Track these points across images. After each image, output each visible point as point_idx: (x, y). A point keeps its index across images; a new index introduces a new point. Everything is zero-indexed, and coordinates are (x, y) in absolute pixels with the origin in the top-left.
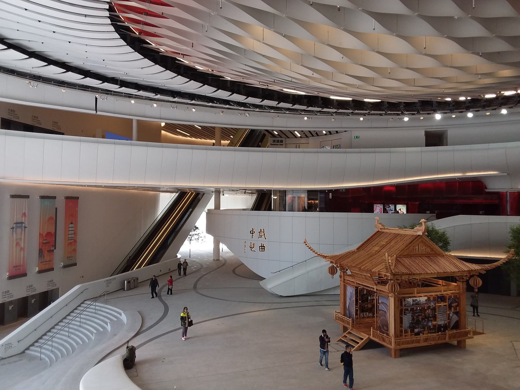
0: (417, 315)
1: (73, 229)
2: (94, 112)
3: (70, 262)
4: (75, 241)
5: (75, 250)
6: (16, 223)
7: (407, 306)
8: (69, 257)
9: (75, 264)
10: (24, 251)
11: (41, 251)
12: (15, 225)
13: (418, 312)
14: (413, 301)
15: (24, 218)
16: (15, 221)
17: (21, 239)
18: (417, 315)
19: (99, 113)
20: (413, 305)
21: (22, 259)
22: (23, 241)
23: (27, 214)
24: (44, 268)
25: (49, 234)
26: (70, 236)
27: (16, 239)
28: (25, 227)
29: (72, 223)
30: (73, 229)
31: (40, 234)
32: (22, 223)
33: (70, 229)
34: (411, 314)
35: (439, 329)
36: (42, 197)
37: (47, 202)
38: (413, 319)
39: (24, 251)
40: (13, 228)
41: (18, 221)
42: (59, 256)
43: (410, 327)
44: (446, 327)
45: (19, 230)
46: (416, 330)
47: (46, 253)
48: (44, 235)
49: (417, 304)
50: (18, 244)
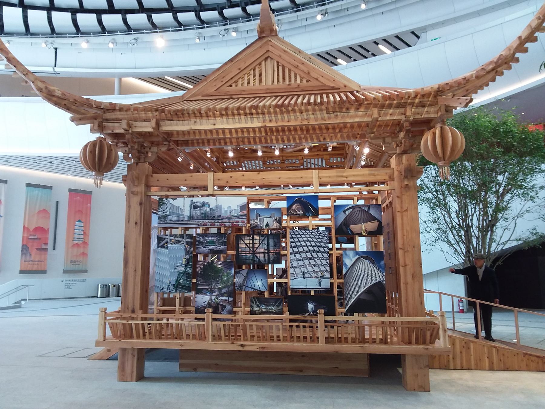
0: (206, 249)
1: (82, 228)
2: (50, 69)
3: (76, 268)
4: (85, 243)
5: (84, 254)
7: (171, 222)
8: (75, 262)
11: (25, 248)
13: (212, 243)
14: (194, 207)
18: (206, 249)
19: (57, 69)
20: (191, 218)
24: (29, 268)
25: (39, 229)
26: (76, 236)
29: (80, 221)
30: (82, 228)
31: (24, 227)
34: (182, 246)
35: (296, 302)
36: (28, 185)
37: (37, 192)
38: (192, 261)
42: (58, 257)
43: (178, 286)
44: (325, 300)
46: (203, 299)
47: (34, 252)
48: (32, 229)
49: (205, 216)
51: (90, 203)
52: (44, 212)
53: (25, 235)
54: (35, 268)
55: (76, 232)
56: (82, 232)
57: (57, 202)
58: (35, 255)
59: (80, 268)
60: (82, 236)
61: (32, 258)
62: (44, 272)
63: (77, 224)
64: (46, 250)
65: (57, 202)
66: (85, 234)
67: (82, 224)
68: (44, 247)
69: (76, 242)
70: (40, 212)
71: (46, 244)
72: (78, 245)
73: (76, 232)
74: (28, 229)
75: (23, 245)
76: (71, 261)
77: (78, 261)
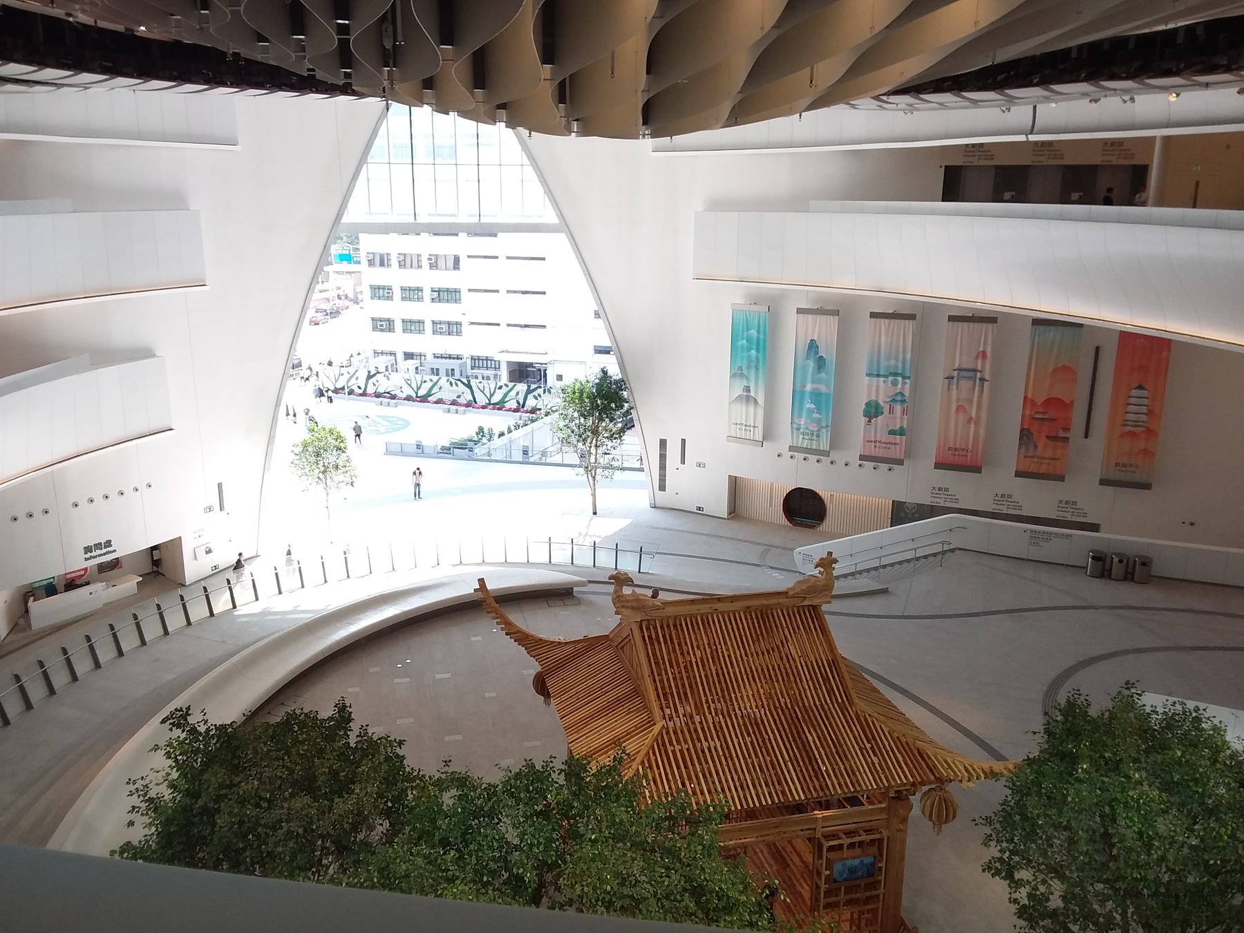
1: (1145, 401)
4: (1150, 432)
6: (960, 370)
8: (1124, 465)
9: (1147, 486)
10: (977, 424)
11: (1026, 435)
12: (955, 373)
15: (980, 362)
16: (956, 366)
17: (971, 401)
21: (971, 439)
22: (975, 405)
23: (989, 355)
24: (1033, 468)
26: (1131, 417)
27: (958, 399)
28: (982, 380)
29: (1140, 387)
30: (1145, 401)
31: (1026, 398)
32: (975, 370)
33: (1132, 400)
37: (1052, 332)
39: (977, 424)
40: (950, 378)
41: (964, 366)
45: (965, 384)
48: (1040, 401)
50: (960, 408)
51: (1169, 351)
52: (1065, 372)
53: (1027, 413)
54: (1043, 469)
55: (1131, 408)
56: (1144, 409)
57: (1098, 348)
58: (1044, 448)
59: (1138, 477)
60: (1144, 418)
61: (1039, 453)
62: (1061, 478)
63: (1134, 392)
64: (1066, 440)
65: (1098, 348)
66: (1150, 413)
67: (1145, 393)
68: (1061, 434)
69: (1128, 429)
70: (1055, 371)
71: (1067, 429)
72: (1133, 435)
73: (1131, 408)
74: (1033, 401)
75: (1022, 430)
76: (1117, 464)
77: (1131, 465)
